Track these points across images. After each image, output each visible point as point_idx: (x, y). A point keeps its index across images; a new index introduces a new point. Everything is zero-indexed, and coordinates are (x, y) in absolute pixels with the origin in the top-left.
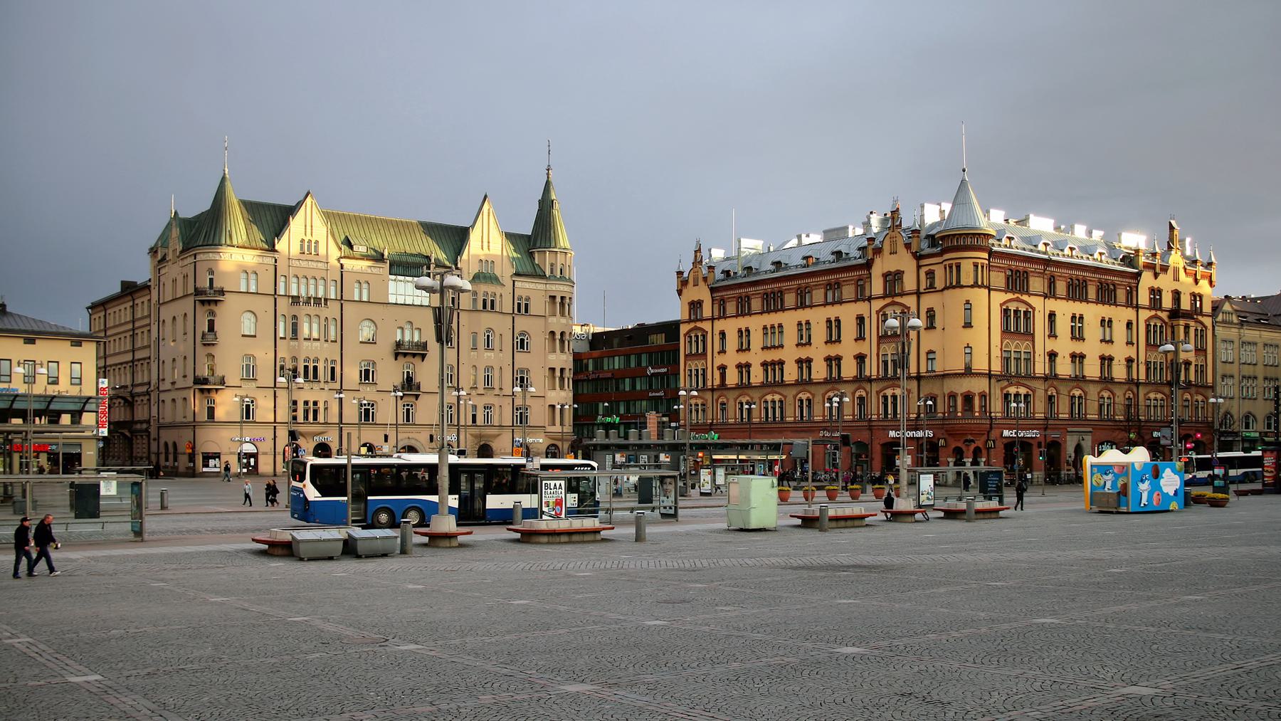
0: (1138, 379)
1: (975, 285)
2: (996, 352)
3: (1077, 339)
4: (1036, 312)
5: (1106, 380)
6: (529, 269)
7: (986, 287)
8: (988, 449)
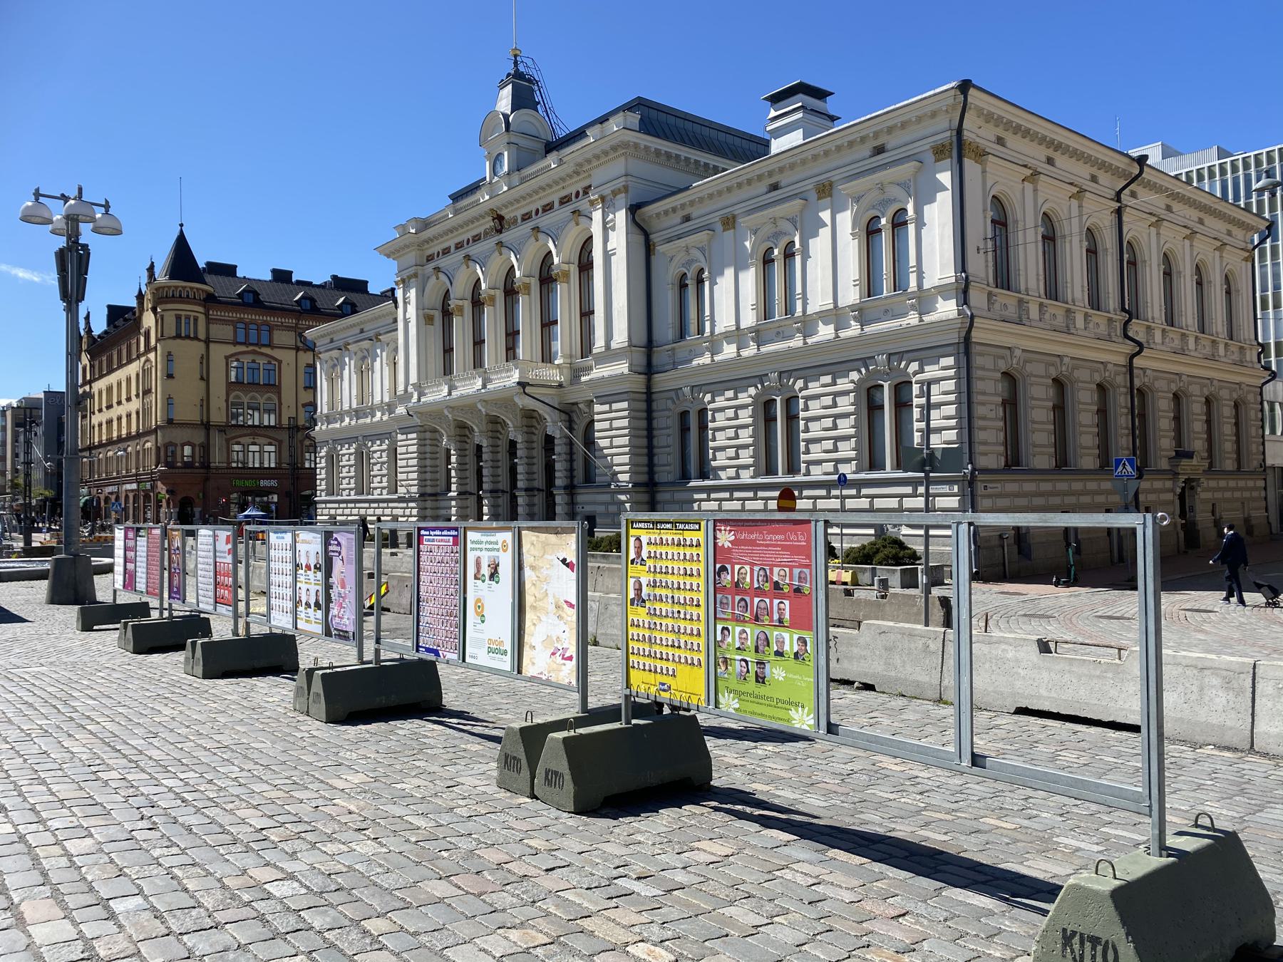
1: (178, 336)
7: (199, 340)
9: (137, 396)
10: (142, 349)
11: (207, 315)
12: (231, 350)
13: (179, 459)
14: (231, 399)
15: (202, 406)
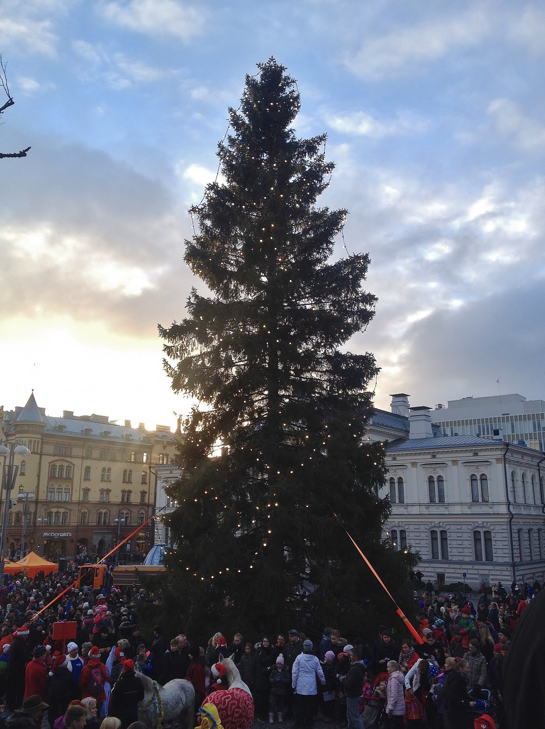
0: (149, 503)
2: (43, 488)
3: (105, 481)
5: (126, 503)
7: (39, 454)
8: (32, 543)
11: (42, 439)
12: (52, 459)
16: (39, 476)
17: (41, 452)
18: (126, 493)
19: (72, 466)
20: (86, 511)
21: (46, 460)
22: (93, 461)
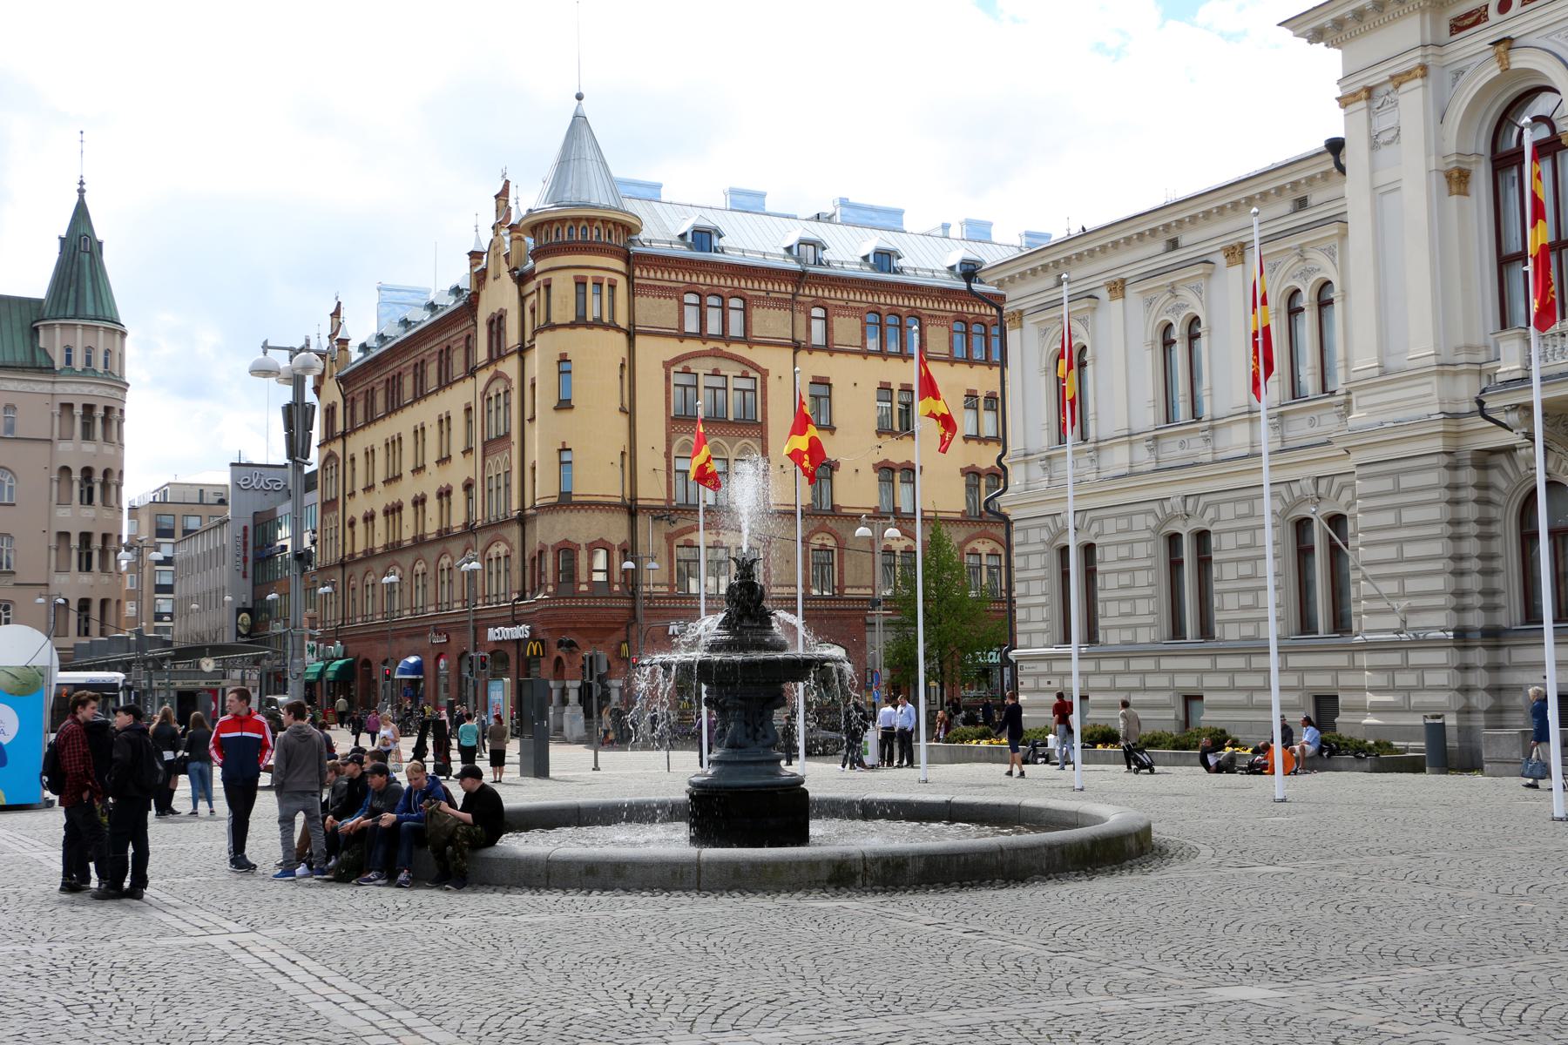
1: (580, 322)
4: (771, 380)
6: (20, 357)
7: (618, 329)
9: (468, 451)
10: (482, 354)
11: (630, 278)
12: (674, 348)
13: (583, 577)
14: (674, 452)
15: (622, 466)
16: (629, 411)
17: (632, 323)
18: (983, 481)
19: (758, 376)
20: (831, 543)
21: (653, 353)
22: (839, 358)
